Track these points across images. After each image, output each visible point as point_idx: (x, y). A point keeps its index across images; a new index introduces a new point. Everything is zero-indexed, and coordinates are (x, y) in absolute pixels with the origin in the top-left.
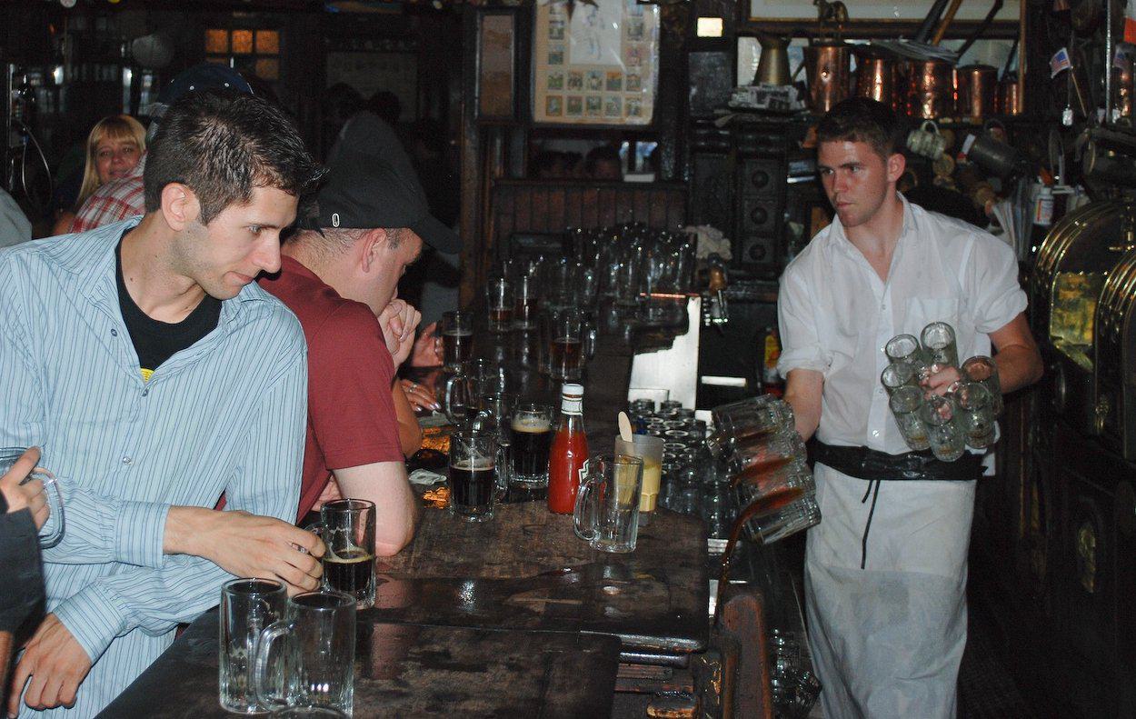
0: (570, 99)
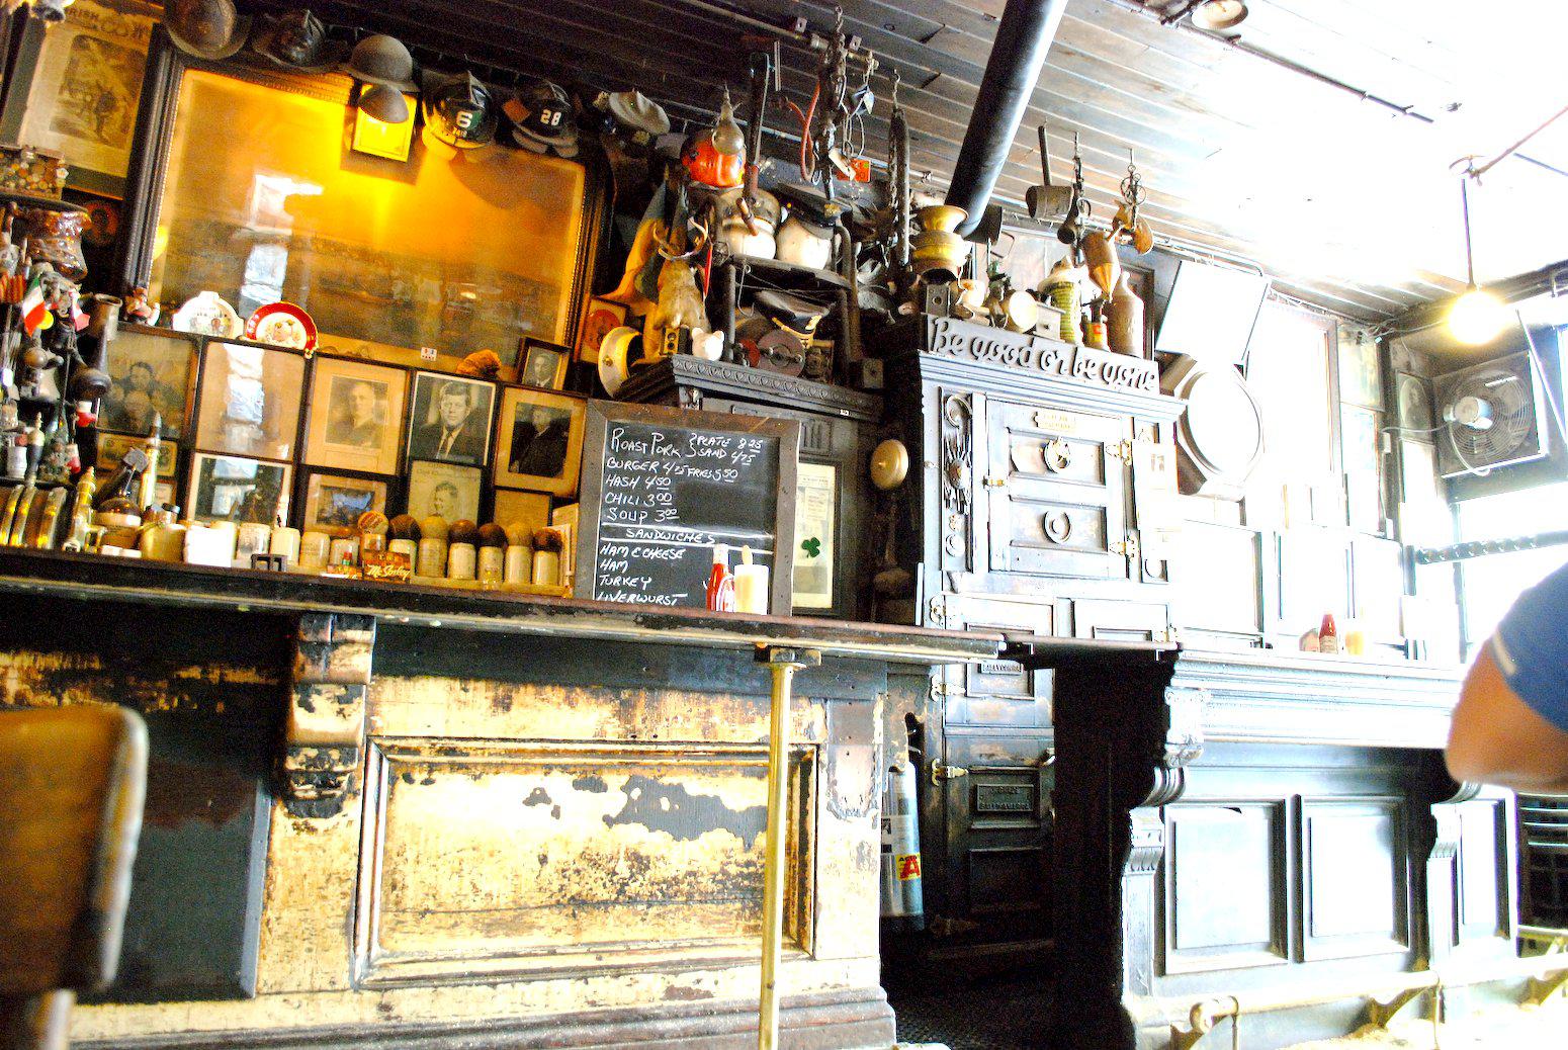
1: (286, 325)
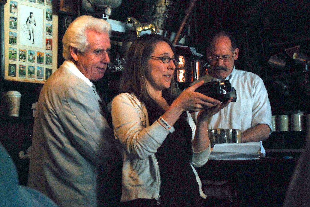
0: (20, 66)
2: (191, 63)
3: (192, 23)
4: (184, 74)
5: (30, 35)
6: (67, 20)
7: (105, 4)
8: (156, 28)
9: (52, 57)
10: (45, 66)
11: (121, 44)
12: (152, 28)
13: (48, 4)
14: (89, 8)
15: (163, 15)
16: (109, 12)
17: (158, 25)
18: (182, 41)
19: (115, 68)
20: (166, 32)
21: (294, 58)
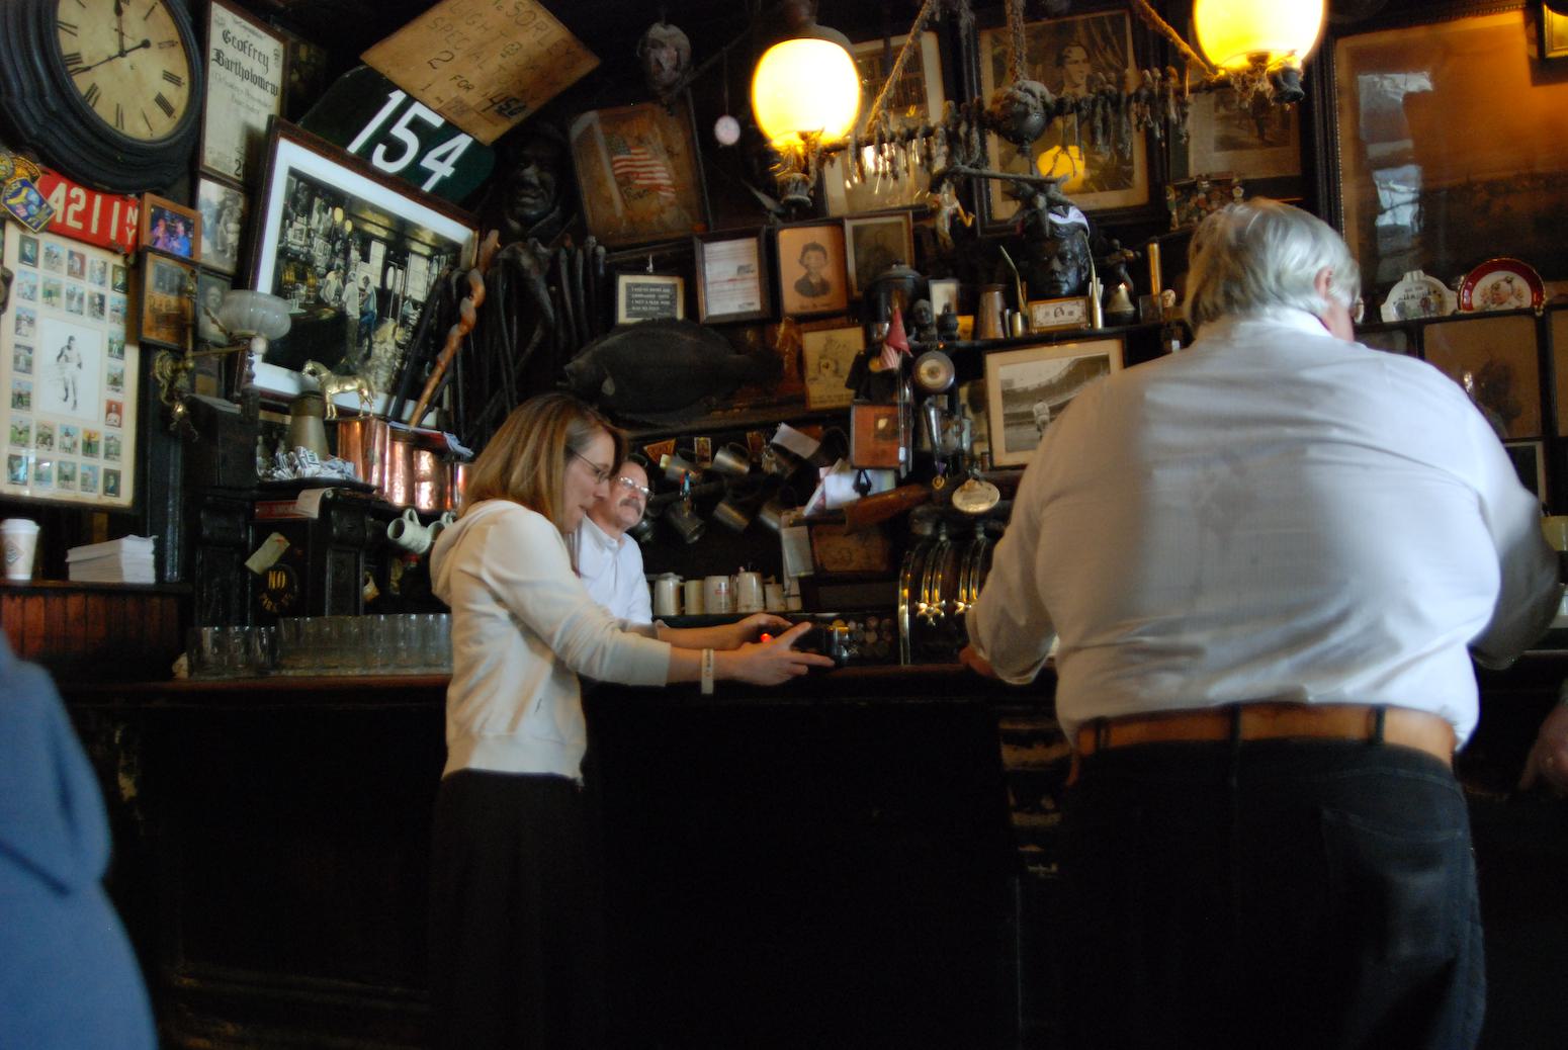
1: (1504, 285)
2: (448, 468)
3: (453, 383)
4: (431, 493)
5: (67, 390)
6: (161, 359)
7: (251, 328)
8: (370, 389)
9: (119, 442)
10: (101, 464)
11: (288, 419)
12: (360, 391)
13: (113, 319)
14: (215, 336)
15: (389, 360)
16: (260, 346)
17: (376, 383)
18: (430, 420)
19: (273, 472)
20: (395, 398)
21: (662, 465)
